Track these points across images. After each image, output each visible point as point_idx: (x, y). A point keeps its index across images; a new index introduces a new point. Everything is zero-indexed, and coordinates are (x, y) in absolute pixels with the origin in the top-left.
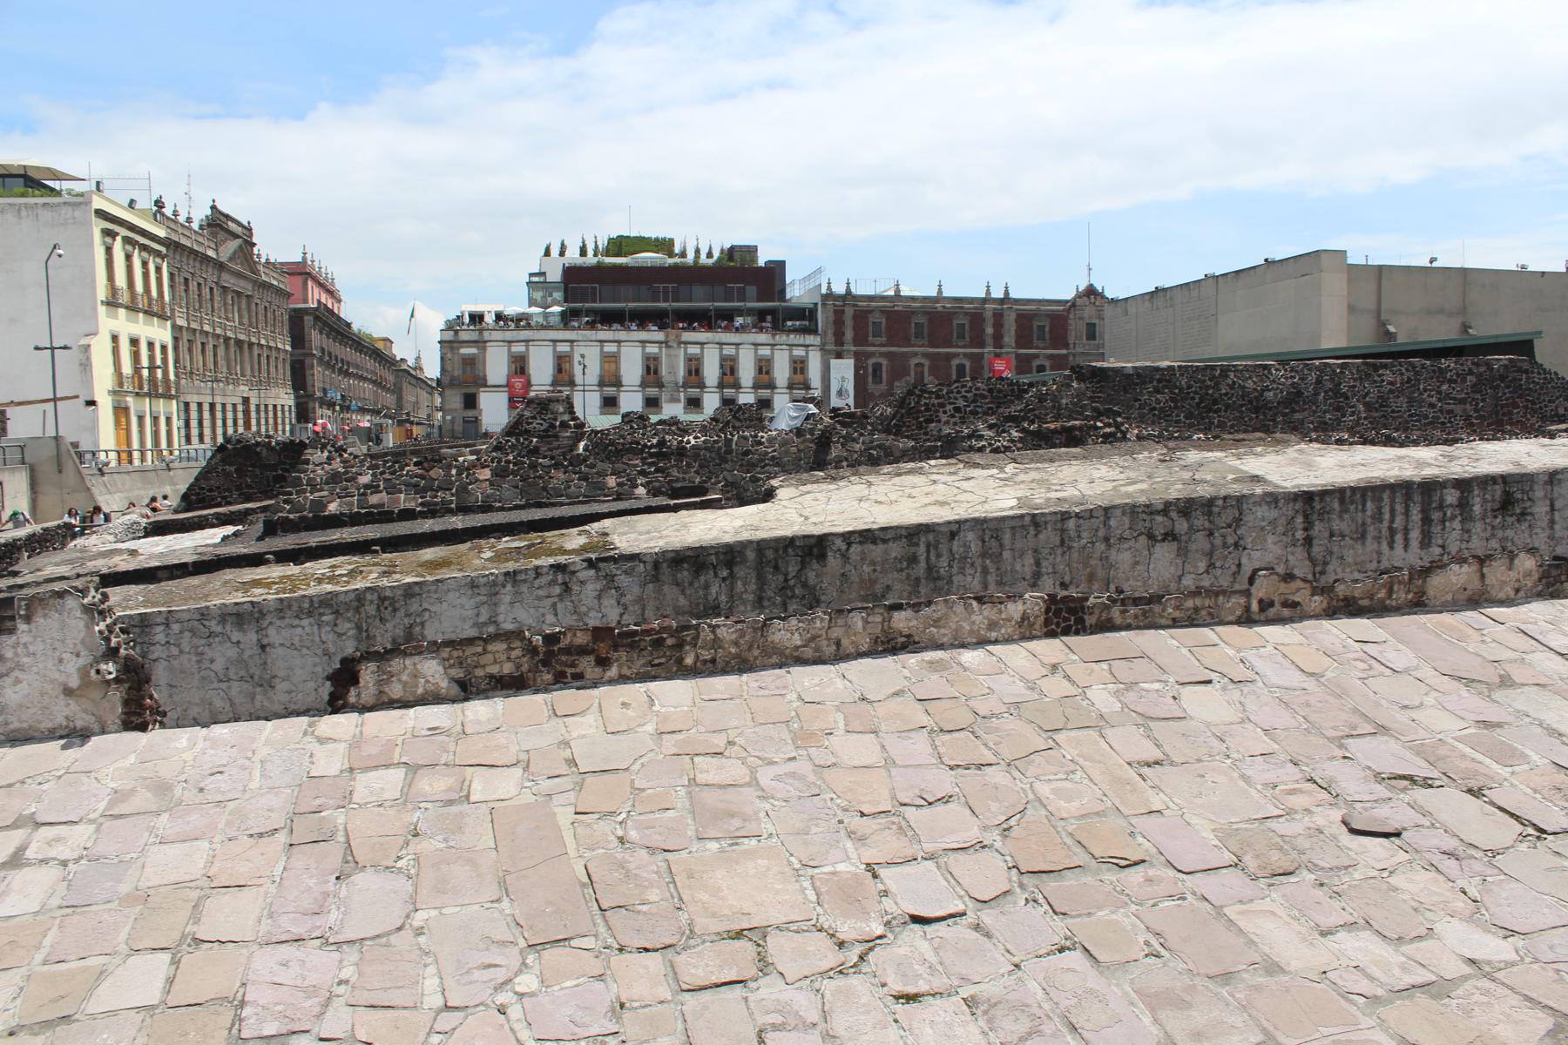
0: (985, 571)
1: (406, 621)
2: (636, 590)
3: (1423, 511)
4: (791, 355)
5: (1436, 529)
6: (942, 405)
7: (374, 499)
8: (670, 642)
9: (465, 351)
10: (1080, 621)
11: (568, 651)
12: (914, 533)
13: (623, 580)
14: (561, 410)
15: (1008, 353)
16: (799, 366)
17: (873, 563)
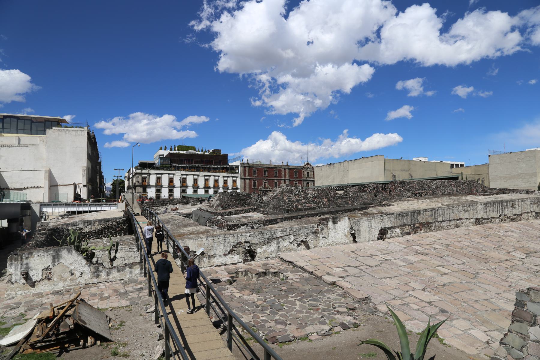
0: (442, 217)
1: (357, 227)
2: (393, 220)
3: (502, 207)
4: (232, 179)
5: (504, 210)
6: (368, 189)
7: (307, 205)
8: (430, 226)
9: (144, 176)
10: (480, 223)
11: (416, 228)
12: (433, 210)
13: (392, 219)
14: (300, 188)
15: (288, 180)
16: (234, 182)
17: (427, 216)
